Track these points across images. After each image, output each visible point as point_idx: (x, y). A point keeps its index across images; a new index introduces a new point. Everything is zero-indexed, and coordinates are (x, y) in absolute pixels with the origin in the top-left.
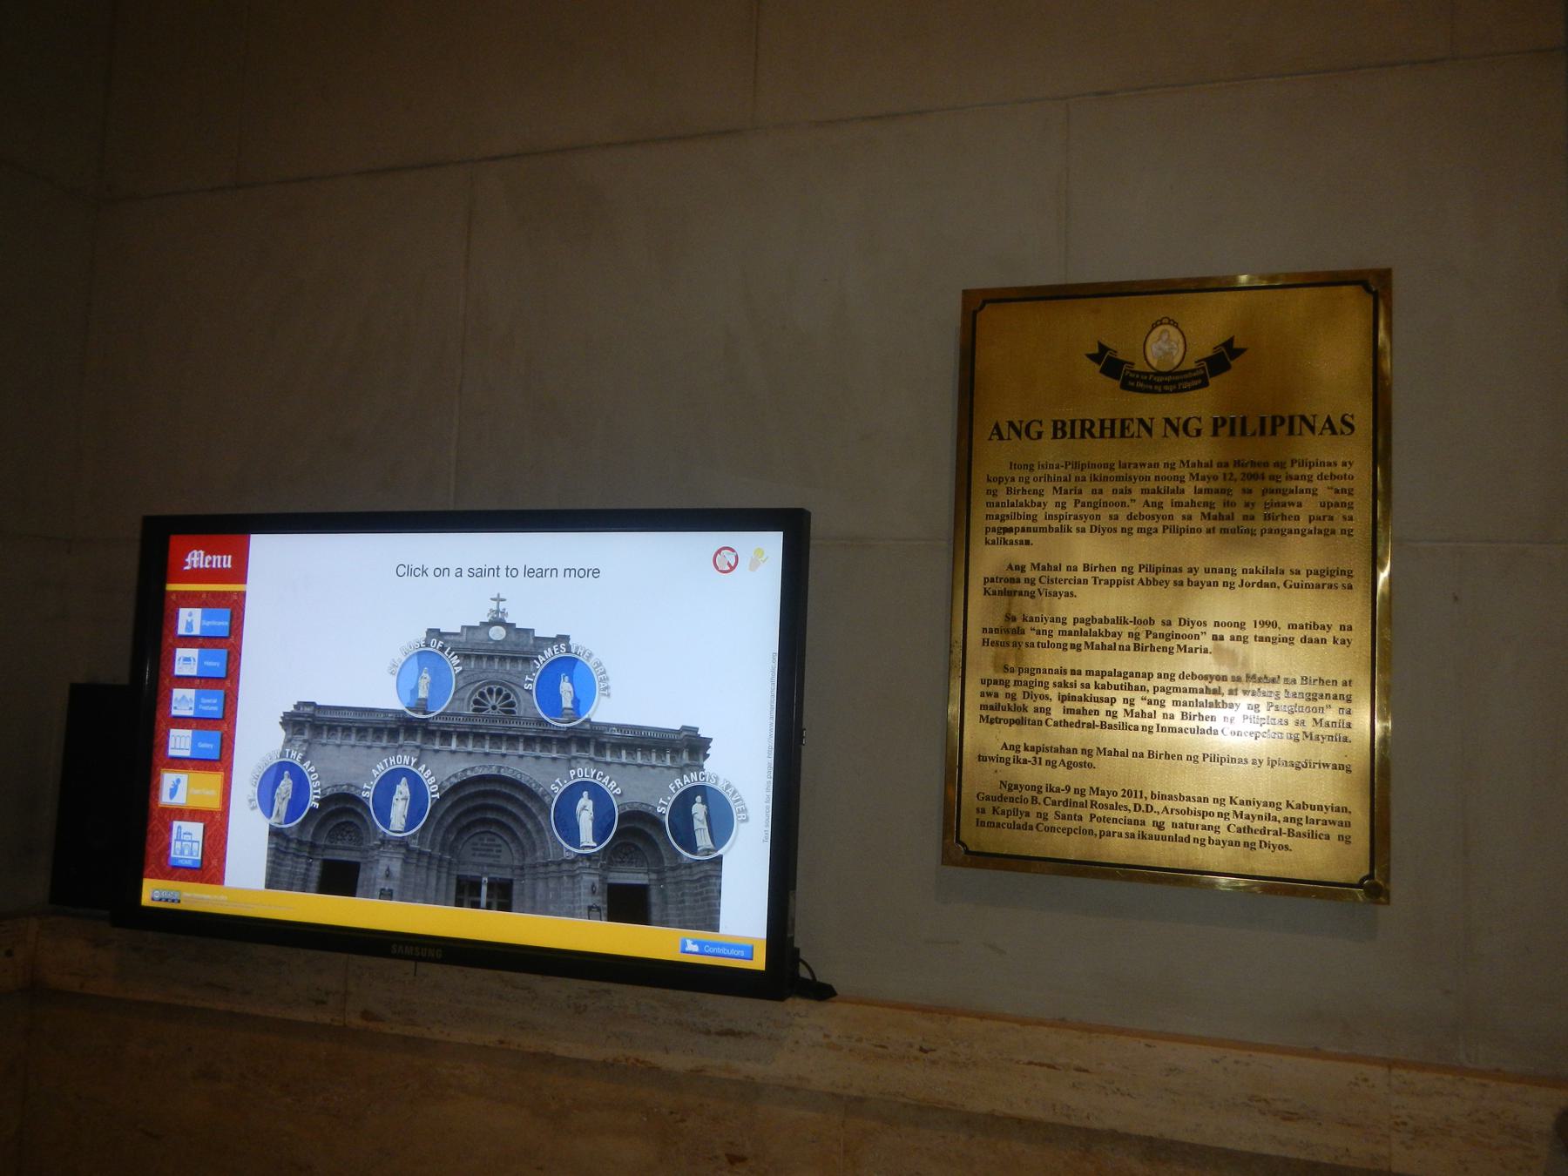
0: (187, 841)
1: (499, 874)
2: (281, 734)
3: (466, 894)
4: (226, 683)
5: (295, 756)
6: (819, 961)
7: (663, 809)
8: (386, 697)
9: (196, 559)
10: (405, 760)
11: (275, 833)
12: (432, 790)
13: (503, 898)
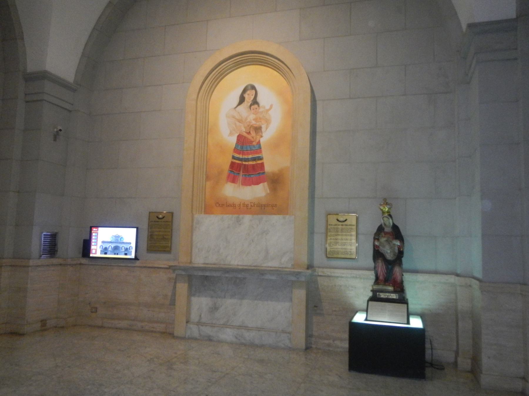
0: (94, 251)
1: (117, 253)
2: (101, 243)
3: (115, 254)
4: (97, 239)
5: (102, 245)
6: (138, 257)
7: (128, 248)
8: (110, 240)
9: (94, 229)
10: (110, 245)
11: (101, 250)
12: (113, 247)
13: (117, 254)
